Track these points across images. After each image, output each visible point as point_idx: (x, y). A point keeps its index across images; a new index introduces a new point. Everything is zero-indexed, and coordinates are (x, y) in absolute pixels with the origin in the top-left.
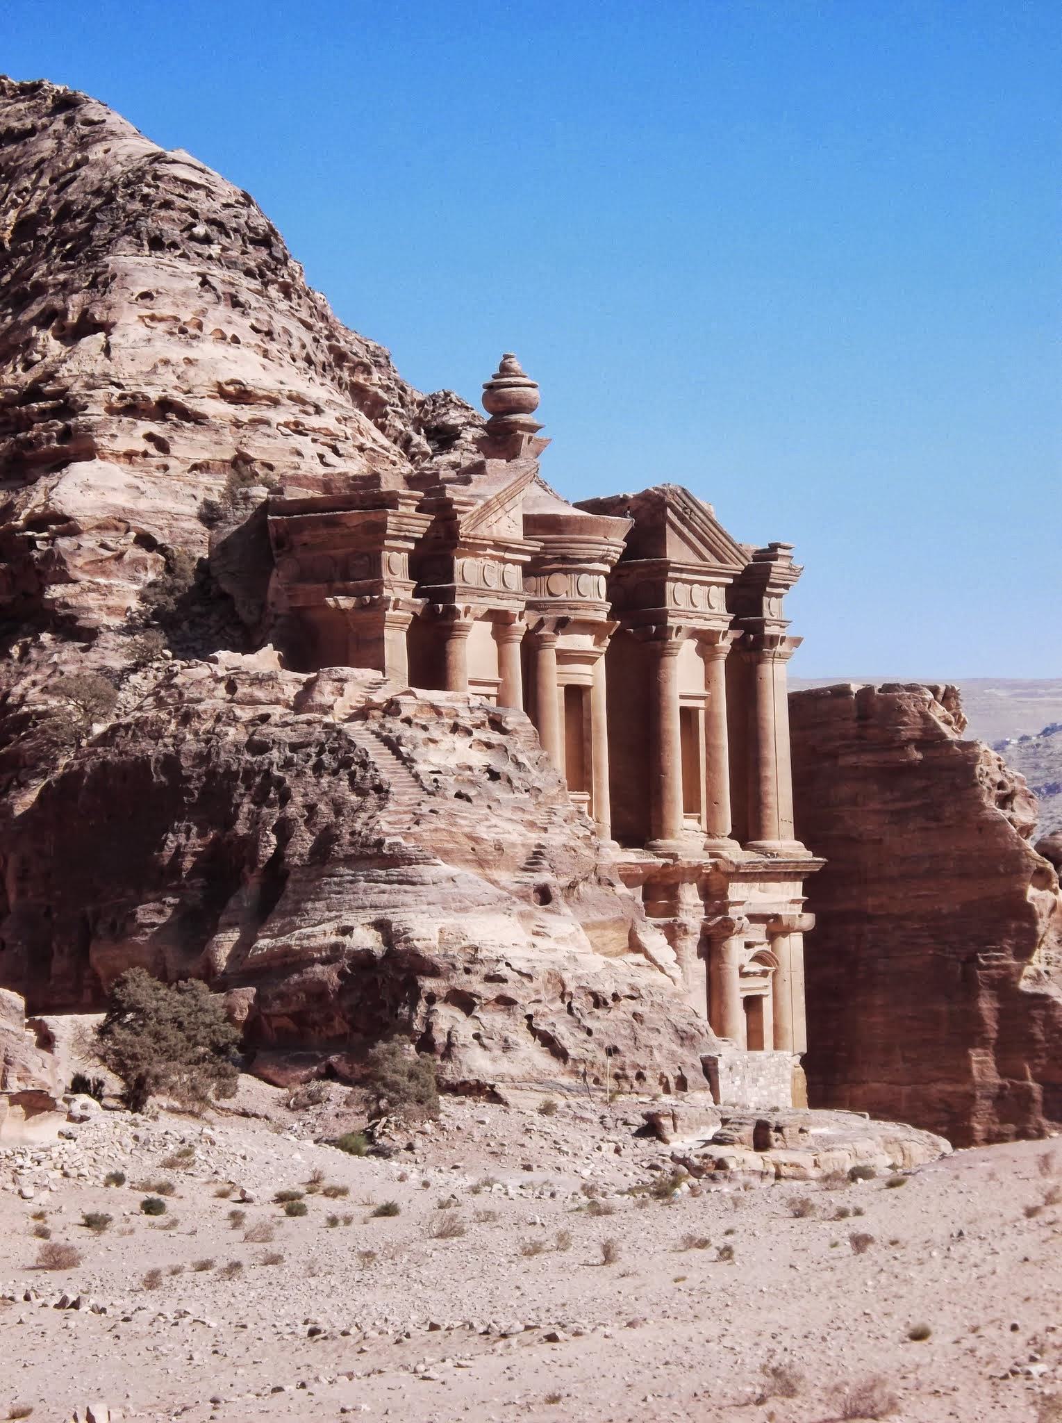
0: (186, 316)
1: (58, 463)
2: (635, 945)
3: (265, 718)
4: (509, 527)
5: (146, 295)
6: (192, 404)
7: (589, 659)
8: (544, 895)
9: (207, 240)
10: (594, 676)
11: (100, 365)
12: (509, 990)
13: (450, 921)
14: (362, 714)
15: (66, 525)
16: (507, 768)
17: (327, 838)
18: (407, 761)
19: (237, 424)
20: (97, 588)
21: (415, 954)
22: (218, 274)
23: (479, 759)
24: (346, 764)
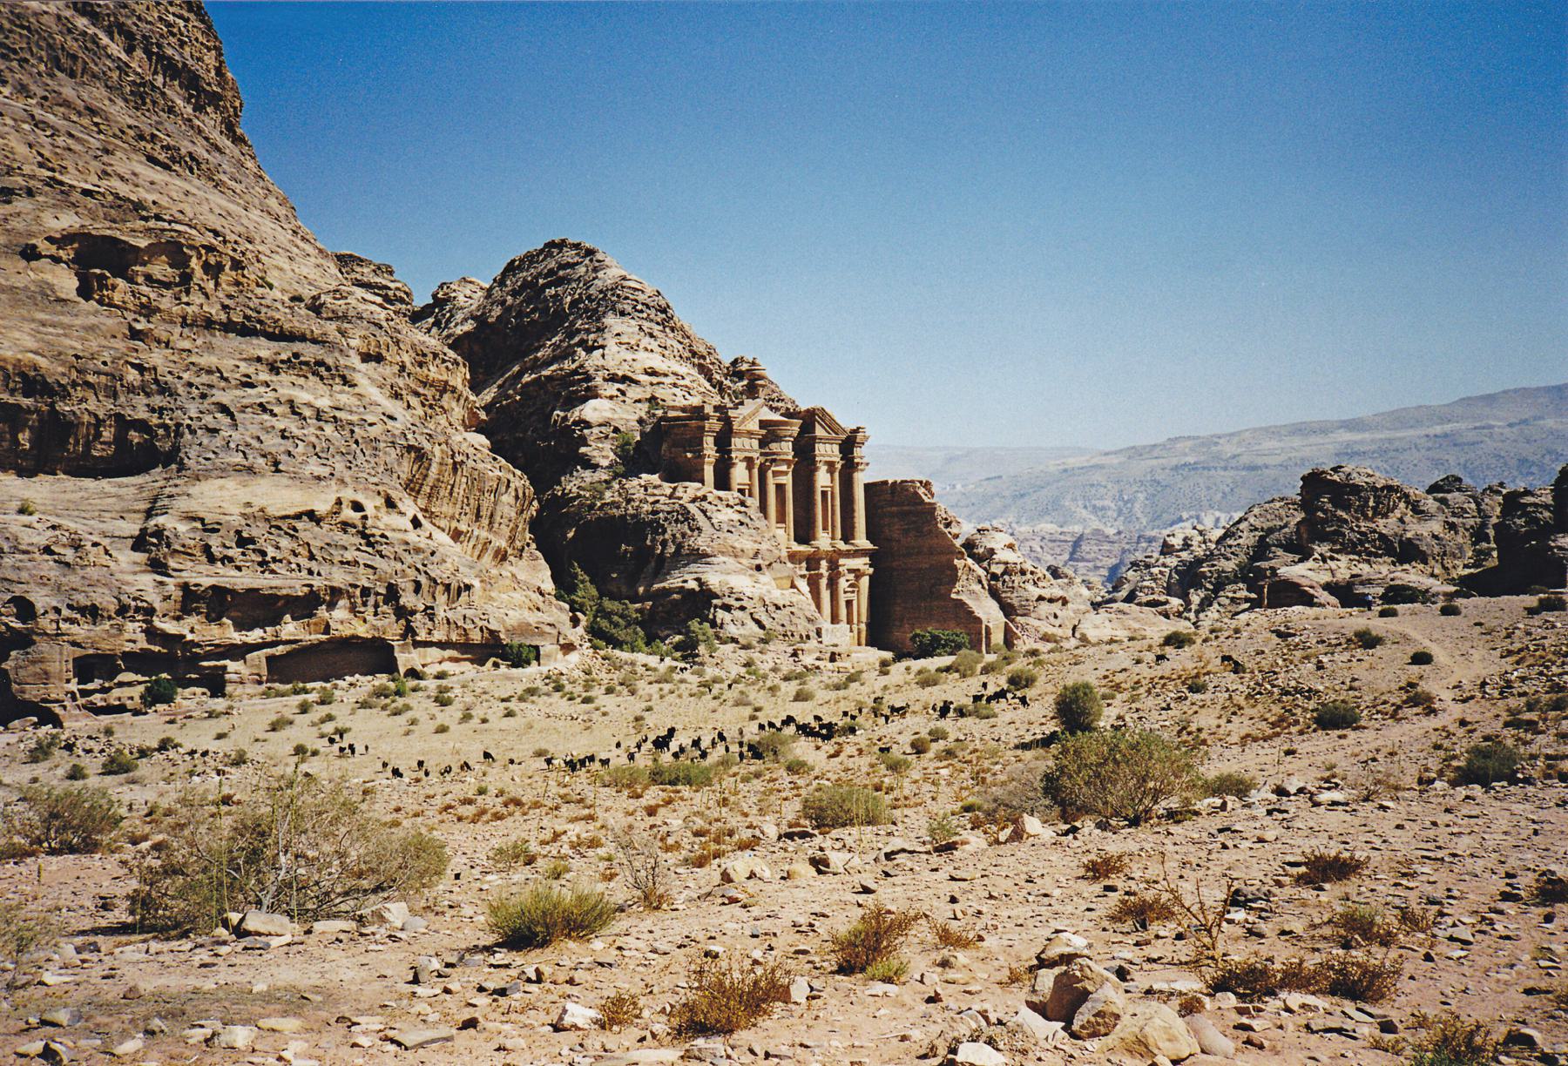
0: (633, 342)
1: (584, 400)
2: (793, 586)
3: (658, 501)
4: (753, 426)
5: (618, 335)
6: (634, 377)
7: (785, 473)
8: (758, 568)
9: (642, 311)
10: (787, 480)
11: (601, 362)
12: (743, 603)
13: (723, 578)
14: (693, 501)
15: (588, 425)
16: (747, 520)
17: (679, 547)
18: (709, 518)
19: (652, 384)
20: (598, 448)
21: (710, 590)
22: (646, 325)
23: (737, 517)
24: (686, 519)
